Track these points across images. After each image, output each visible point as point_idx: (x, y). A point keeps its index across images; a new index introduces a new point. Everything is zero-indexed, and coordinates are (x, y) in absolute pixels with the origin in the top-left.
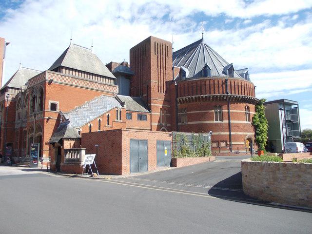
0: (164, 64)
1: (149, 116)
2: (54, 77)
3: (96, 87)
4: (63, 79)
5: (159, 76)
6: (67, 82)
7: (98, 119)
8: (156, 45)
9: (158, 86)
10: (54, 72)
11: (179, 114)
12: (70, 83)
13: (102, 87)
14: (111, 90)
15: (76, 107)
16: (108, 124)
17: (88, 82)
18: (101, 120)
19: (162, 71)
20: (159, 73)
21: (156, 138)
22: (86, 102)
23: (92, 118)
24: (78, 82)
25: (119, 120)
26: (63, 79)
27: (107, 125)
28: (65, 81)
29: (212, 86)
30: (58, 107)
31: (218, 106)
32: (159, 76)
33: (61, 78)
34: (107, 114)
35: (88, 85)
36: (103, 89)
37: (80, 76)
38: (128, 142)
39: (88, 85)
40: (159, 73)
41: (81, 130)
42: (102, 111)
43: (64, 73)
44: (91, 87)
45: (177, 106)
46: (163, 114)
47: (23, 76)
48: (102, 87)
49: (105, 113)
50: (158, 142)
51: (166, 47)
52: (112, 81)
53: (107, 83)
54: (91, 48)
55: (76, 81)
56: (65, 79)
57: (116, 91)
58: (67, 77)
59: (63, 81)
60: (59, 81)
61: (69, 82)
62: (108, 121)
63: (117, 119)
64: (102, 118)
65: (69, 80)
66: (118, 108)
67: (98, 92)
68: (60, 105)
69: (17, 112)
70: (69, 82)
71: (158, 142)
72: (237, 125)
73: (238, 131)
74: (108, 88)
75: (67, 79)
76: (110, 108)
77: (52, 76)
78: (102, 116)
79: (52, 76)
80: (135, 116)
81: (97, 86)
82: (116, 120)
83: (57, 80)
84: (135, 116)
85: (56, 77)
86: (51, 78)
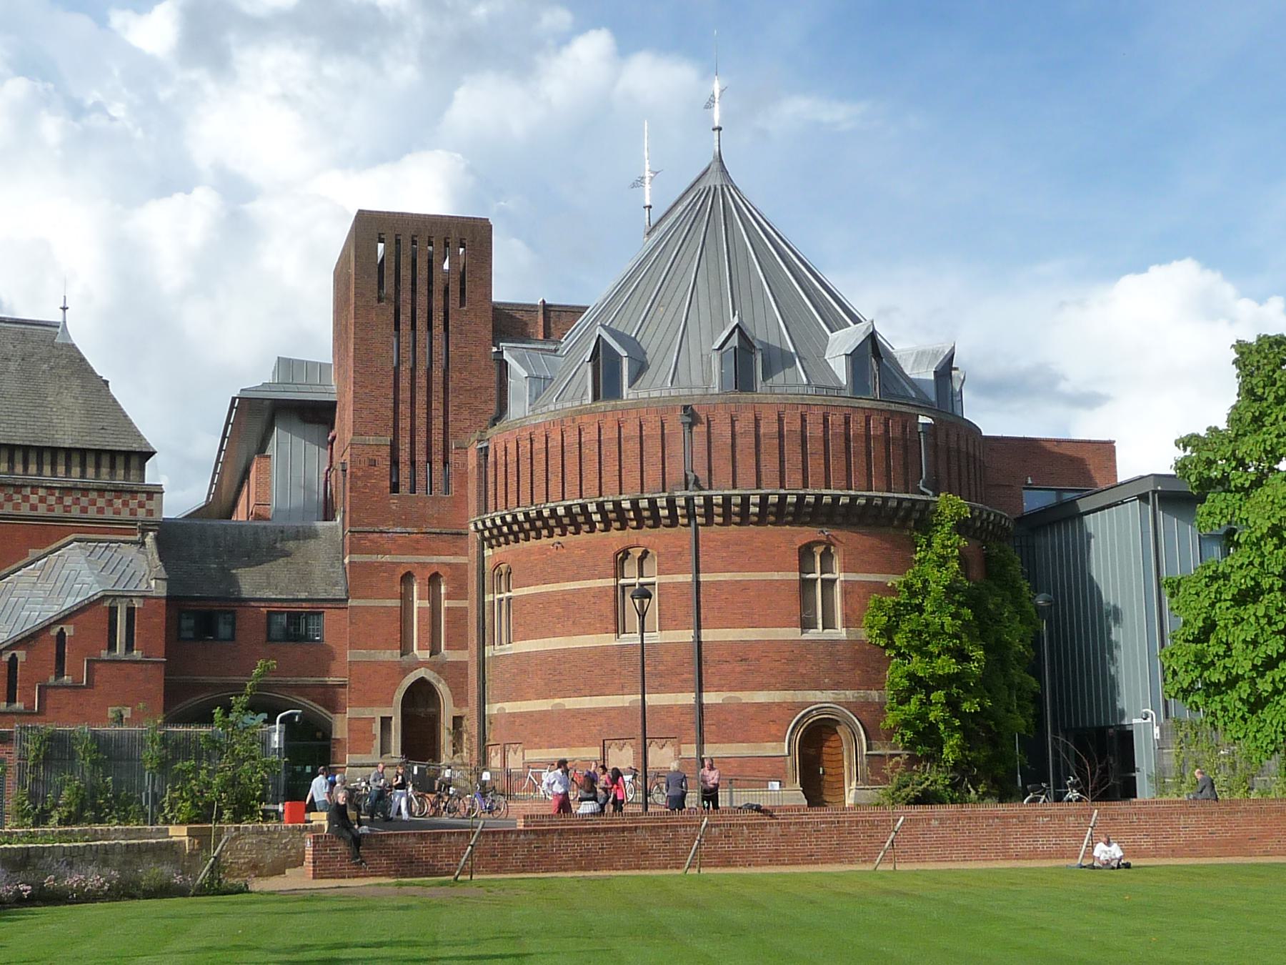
5: (404, 408)
9: (395, 462)
11: (488, 598)
16: (60, 672)
19: (422, 381)
20: (405, 395)
29: (610, 449)
34: (55, 631)
36: (75, 511)
40: (405, 395)
45: (482, 558)
48: (68, 501)
49: (46, 629)
54: (54, 316)
63: (112, 646)
72: (742, 652)
74: (101, 502)
78: (28, 640)
81: (42, 500)
82: (104, 654)
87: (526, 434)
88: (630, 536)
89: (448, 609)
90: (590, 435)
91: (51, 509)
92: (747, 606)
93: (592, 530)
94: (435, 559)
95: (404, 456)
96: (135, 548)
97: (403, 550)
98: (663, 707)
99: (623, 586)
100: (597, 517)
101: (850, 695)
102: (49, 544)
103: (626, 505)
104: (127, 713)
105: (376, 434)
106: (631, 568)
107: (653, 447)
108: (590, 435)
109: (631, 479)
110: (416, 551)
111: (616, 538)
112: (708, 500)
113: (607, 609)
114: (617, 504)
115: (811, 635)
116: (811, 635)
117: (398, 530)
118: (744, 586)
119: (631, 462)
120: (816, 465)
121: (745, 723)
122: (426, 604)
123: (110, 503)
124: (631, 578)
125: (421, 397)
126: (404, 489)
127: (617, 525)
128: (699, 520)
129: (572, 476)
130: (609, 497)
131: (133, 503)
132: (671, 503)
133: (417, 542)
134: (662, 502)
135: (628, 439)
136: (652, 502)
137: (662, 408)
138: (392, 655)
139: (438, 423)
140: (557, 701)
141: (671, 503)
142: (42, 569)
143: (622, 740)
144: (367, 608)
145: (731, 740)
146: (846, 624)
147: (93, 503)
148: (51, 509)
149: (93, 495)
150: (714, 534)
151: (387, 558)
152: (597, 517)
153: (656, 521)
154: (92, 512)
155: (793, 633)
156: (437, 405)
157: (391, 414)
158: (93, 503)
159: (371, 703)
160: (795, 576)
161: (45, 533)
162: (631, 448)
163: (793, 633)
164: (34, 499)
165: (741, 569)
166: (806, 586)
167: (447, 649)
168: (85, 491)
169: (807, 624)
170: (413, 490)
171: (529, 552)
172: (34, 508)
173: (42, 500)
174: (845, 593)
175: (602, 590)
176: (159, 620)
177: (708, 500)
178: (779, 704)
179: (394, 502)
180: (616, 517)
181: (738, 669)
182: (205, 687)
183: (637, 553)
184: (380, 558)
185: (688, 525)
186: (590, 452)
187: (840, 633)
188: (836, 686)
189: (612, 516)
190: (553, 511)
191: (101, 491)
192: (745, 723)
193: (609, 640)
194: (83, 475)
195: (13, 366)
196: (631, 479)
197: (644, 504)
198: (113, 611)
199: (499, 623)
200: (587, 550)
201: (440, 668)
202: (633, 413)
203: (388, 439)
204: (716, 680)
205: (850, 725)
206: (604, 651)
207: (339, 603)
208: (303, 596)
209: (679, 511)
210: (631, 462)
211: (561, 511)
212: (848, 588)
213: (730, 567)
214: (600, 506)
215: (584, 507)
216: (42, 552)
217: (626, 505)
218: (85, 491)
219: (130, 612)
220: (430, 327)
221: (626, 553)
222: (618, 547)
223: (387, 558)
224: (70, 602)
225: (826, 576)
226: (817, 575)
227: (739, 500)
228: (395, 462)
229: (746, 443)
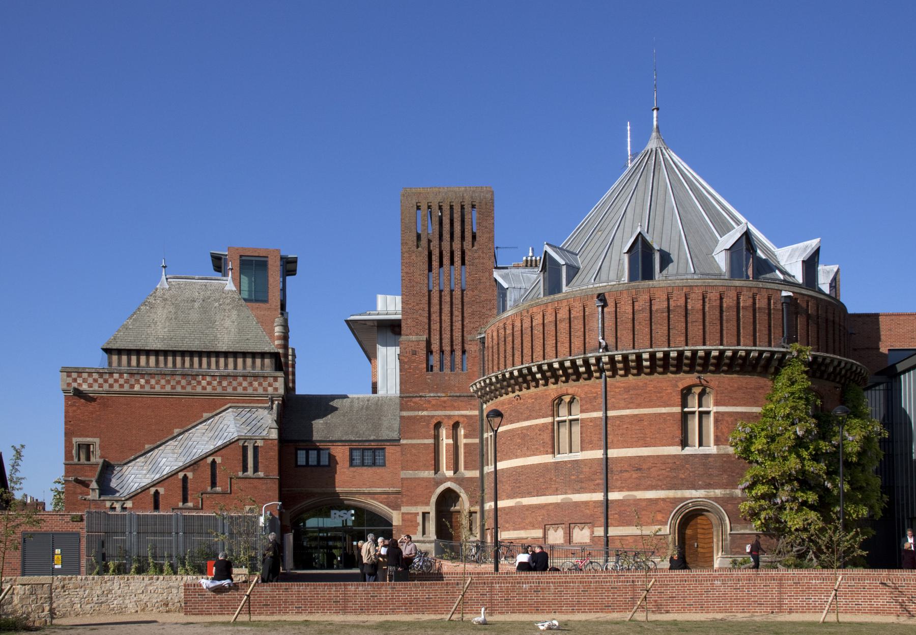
2: (80, 381)
3: (204, 388)
4: (106, 381)
5: (435, 317)
6: (116, 388)
9: (429, 351)
12: (126, 388)
13: (225, 383)
17: (178, 378)
20: (435, 308)
24: (147, 382)
26: (106, 381)
28: (111, 386)
29: (550, 328)
32: (435, 317)
33: (101, 381)
35: (182, 386)
36: (230, 390)
37: (162, 365)
39: (182, 386)
40: (435, 308)
44: (189, 389)
48: (225, 383)
52: (267, 361)
53: (249, 369)
55: (142, 381)
56: (111, 381)
57: (276, 389)
58: (116, 376)
59: (106, 387)
60: (96, 387)
61: (121, 386)
65: (121, 381)
70: (121, 386)
72: (637, 464)
73: (637, 488)
74: (245, 384)
75: (116, 381)
77: (75, 380)
79: (75, 380)
81: (209, 383)
83: (90, 386)
85: (85, 381)
86: (75, 385)
87: (501, 325)
88: (561, 387)
89: (465, 445)
90: (538, 320)
91: (214, 388)
92: (642, 432)
93: (537, 386)
94: (456, 413)
95: (435, 347)
96: (266, 412)
97: (436, 407)
98: (583, 502)
99: (559, 422)
100: (539, 376)
101: (718, 492)
102: (215, 410)
105: (417, 334)
106: (563, 410)
107: (577, 325)
109: (563, 349)
110: (444, 408)
111: (553, 389)
112: (612, 358)
113: (547, 437)
115: (688, 451)
116: (688, 451)
117: (432, 395)
118: (639, 418)
119: (563, 337)
121: (636, 513)
122: (451, 441)
123: (251, 384)
124: (564, 415)
125: (446, 309)
127: (553, 380)
128: (608, 373)
129: (527, 351)
131: (265, 384)
132: (586, 362)
133: (445, 402)
134: (579, 362)
135: (561, 321)
136: (573, 362)
137: (584, 299)
139: (458, 325)
141: (586, 362)
142: (210, 425)
144: (413, 445)
145: (628, 524)
146: (717, 442)
147: (240, 384)
148: (214, 388)
149: (240, 379)
150: (619, 382)
151: (425, 413)
152: (539, 376)
153: (578, 376)
154: (240, 390)
155: (675, 450)
156: (457, 313)
157: (426, 321)
158: (240, 384)
160: (678, 409)
161: (214, 404)
162: (563, 326)
163: (675, 450)
164: (204, 383)
165: (639, 406)
166: (685, 417)
167: (466, 468)
168: (235, 377)
169: (684, 443)
170: (441, 369)
172: (204, 388)
173: (209, 383)
174: (716, 421)
175: (544, 425)
176: (274, 454)
177: (612, 358)
178: (664, 500)
179: (429, 376)
180: (551, 375)
181: (635, 476)
183: (567, 399)
184: (420, 413)
185: (600, 377)
186: (538, 332)
187: (712, 449)
189: (548, 374)
190: (511, 373)
191: (245, 377)
192: (636, 513)
193: (548, 459)
194: (235, 367)
195: (197, 305)
196: (563, 349)
197: (568, 364)
198: (245, 449)
200: (536, 399)
202: (565, 303)
203: (425, 337)
204: (618, 483)
205: (718, 513)
206: (545, 466)
207: (395, 442)
208: (372, 438)
209: (593, 368)
210: (563, 337)
212: (719, 417)
213: (631, 405)
216: (211, 415)
218: (235, 377)
219: (256, 448)
221: (560, 399)
222: (554, 395)
223: (425, 413)
224: (220, 443)
225: (701, 409)
226: (696, 409)
227: (634, 357)
228: (429, 351)
229: (642, 317)
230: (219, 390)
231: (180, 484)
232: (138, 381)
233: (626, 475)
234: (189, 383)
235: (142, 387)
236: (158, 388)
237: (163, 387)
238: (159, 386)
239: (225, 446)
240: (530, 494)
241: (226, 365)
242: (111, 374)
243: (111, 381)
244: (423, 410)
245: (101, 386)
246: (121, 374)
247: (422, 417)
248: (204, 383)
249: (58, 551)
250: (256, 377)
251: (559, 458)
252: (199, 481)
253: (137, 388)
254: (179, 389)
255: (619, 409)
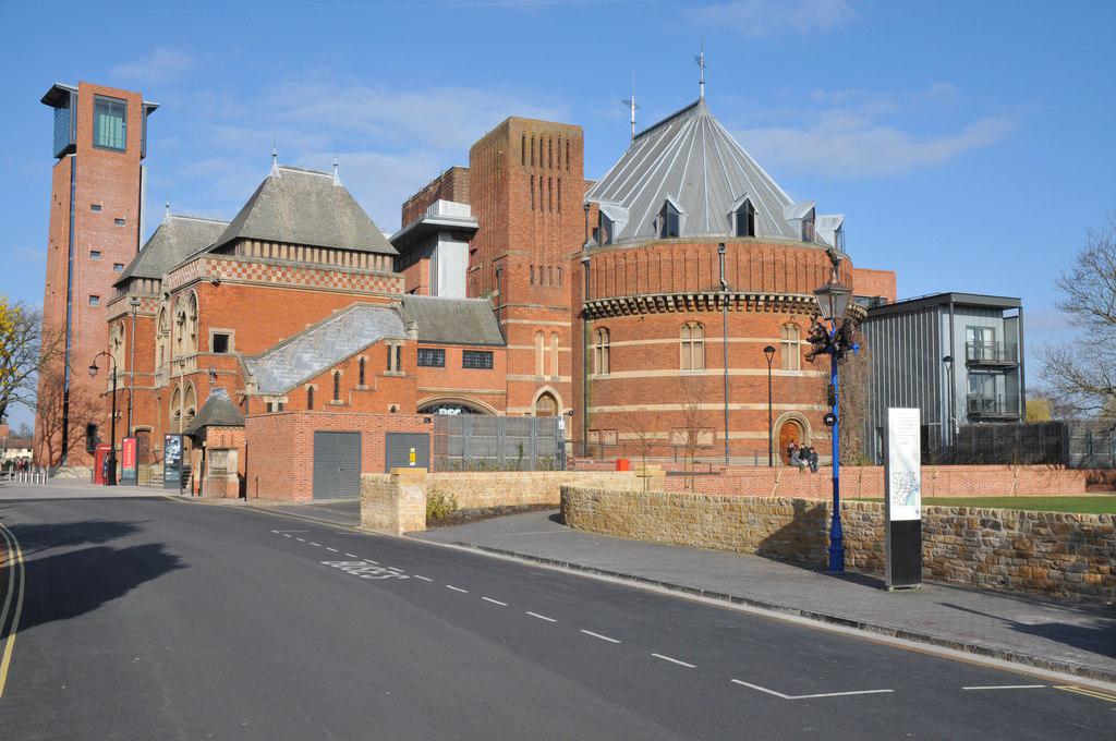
0: (555, 199)
1: (498, 354)
2: (219, 269)
3: (336, 285)
4: (244, 271)
6: (254, 279)
7: (333, 372)
8: (528, 141)
10: (220, 256)
12: (264, 279)
13: (354, 281)
14: (381, 288)
15: (280, 340)
16: (362, 382)
18: (341, 372)
21: (385, 429)
22: (308, 325)
23: (317, 367)
24: (284, 275)
25: (393, 370)
27: (358, 387)
30: (231, 343)
31: (692, 325)
33: (240, 270)
34: (359, 358)
36: (358, 288)
37: (292, 257)
38: (310, 436)
41: (285, 400)
42: (347, 351)
43: (248, 253)
44: (322, 285)
46: (548, 348)
47: (174, 241)
48: (354, 281)
49: (353, 356)
50: (391, 437)
51: (564, 144)
52: (387, 259)
53: (371, 269)
55: (279, 274)
56: (249, 271)
57: (398, 290)
60: (234, 277)
61: (259, 277)
62: (362, 374)
63: (389, 368)
64: (345, 368)
65: (260, 272)
66: (391, 339)
67: (342, 300)
68: (237, 339)
69: (158, 344)
70: (259, 277)
71: (391, 437)
73: (750, 401)
74: (372, 283)
75: (254, 271)
76: (369, 341)
77: (214, 268)
78: (345, 363)
79: (214, 268)
80: (454, 355)
81: (340, 280)
82: (386, 372)
84: (454, 355)
86: (214, 273)
101: (804, 407)
103: (690, 298)
104: (398, 407)
107: (704, 266)
108: (665, 256)
110: (544, 319)
114: (685, 297)
120: (791, 280)
126: (537, 282)
130: (680, 294)
132: (717, 298)
134: (711, 297)
136: (706, 297)
138: (528, 378)
140: (641, 406)
141: (717, 298)
143: (680, 429)
147: (367, 283)
151: (527, 322)
159: (519, 405)
165: (751, 336)
168: (363, 275)
171: (623, 322)
172: (336, 285)
173: (340, 280)
182: (428, 393)
184: (525, 322)
186: (666, 268)
188: (798, 401)
191: (371, 275)
197: (701, 297)
198: (389, 348)
199: (600, 361)
201: (555, 384)
208: (482, 342)
211: (649, 299)
214: (675, 298)
215: (665, 298)
217: (690, 298)
220: (550, 189)
223: (527, 322)
230: (349, 287)
231: (333, 381)
232: (274, 273)
233: (742, 390)
234: (322, 279)
235: (279, 279)
236: (293, 282)
237: (298, 281)
238: (295, 279)
239: (373, 344)
240: (655, 401)
241: (351, 261)
242: (250, 264)
243: (249, 271)
244: (526, 319)
245: (239, 276)
246: (259, 267)
247: (526, 326)
248: (335, 280)
249: (413, 450)
250: (381, 276)
251: (681, 372)
252: (349, 377)
253: (274, 280)
254: (313, 284)
255: (736, 337)
